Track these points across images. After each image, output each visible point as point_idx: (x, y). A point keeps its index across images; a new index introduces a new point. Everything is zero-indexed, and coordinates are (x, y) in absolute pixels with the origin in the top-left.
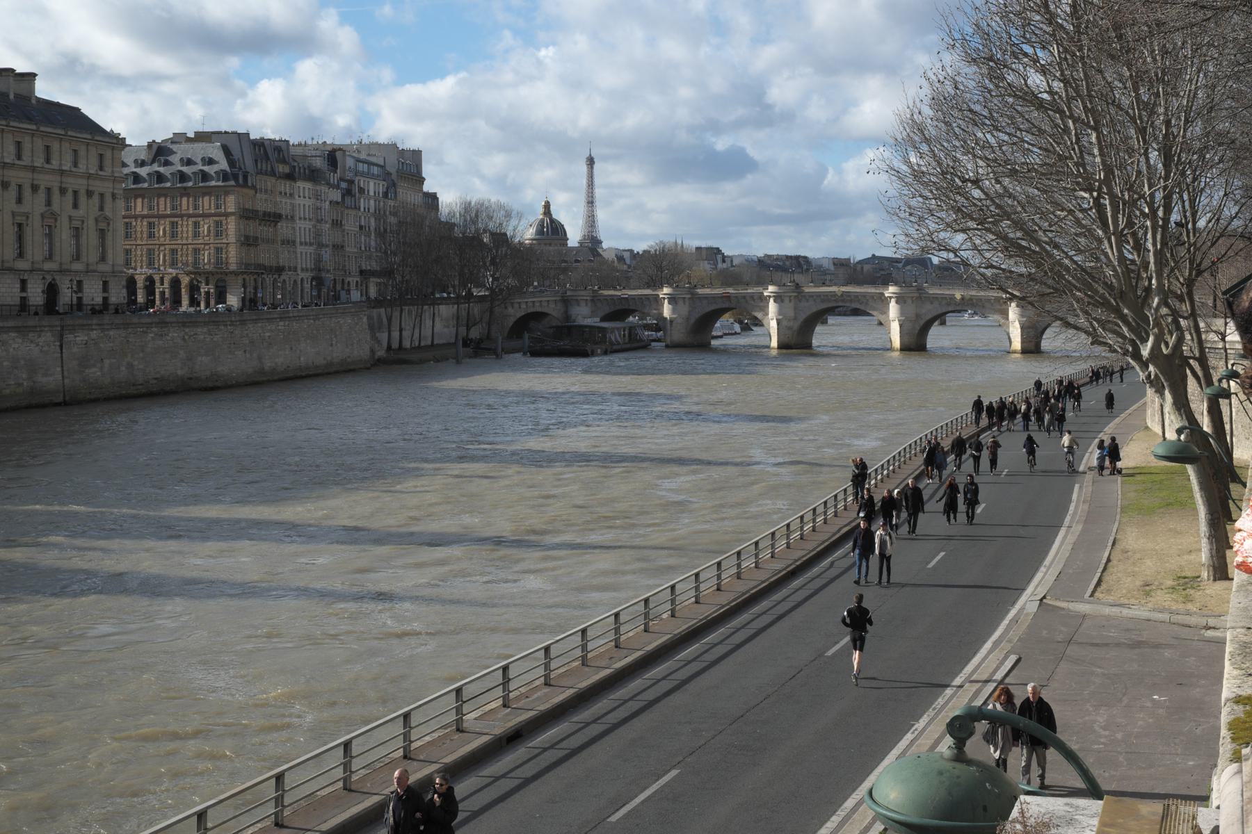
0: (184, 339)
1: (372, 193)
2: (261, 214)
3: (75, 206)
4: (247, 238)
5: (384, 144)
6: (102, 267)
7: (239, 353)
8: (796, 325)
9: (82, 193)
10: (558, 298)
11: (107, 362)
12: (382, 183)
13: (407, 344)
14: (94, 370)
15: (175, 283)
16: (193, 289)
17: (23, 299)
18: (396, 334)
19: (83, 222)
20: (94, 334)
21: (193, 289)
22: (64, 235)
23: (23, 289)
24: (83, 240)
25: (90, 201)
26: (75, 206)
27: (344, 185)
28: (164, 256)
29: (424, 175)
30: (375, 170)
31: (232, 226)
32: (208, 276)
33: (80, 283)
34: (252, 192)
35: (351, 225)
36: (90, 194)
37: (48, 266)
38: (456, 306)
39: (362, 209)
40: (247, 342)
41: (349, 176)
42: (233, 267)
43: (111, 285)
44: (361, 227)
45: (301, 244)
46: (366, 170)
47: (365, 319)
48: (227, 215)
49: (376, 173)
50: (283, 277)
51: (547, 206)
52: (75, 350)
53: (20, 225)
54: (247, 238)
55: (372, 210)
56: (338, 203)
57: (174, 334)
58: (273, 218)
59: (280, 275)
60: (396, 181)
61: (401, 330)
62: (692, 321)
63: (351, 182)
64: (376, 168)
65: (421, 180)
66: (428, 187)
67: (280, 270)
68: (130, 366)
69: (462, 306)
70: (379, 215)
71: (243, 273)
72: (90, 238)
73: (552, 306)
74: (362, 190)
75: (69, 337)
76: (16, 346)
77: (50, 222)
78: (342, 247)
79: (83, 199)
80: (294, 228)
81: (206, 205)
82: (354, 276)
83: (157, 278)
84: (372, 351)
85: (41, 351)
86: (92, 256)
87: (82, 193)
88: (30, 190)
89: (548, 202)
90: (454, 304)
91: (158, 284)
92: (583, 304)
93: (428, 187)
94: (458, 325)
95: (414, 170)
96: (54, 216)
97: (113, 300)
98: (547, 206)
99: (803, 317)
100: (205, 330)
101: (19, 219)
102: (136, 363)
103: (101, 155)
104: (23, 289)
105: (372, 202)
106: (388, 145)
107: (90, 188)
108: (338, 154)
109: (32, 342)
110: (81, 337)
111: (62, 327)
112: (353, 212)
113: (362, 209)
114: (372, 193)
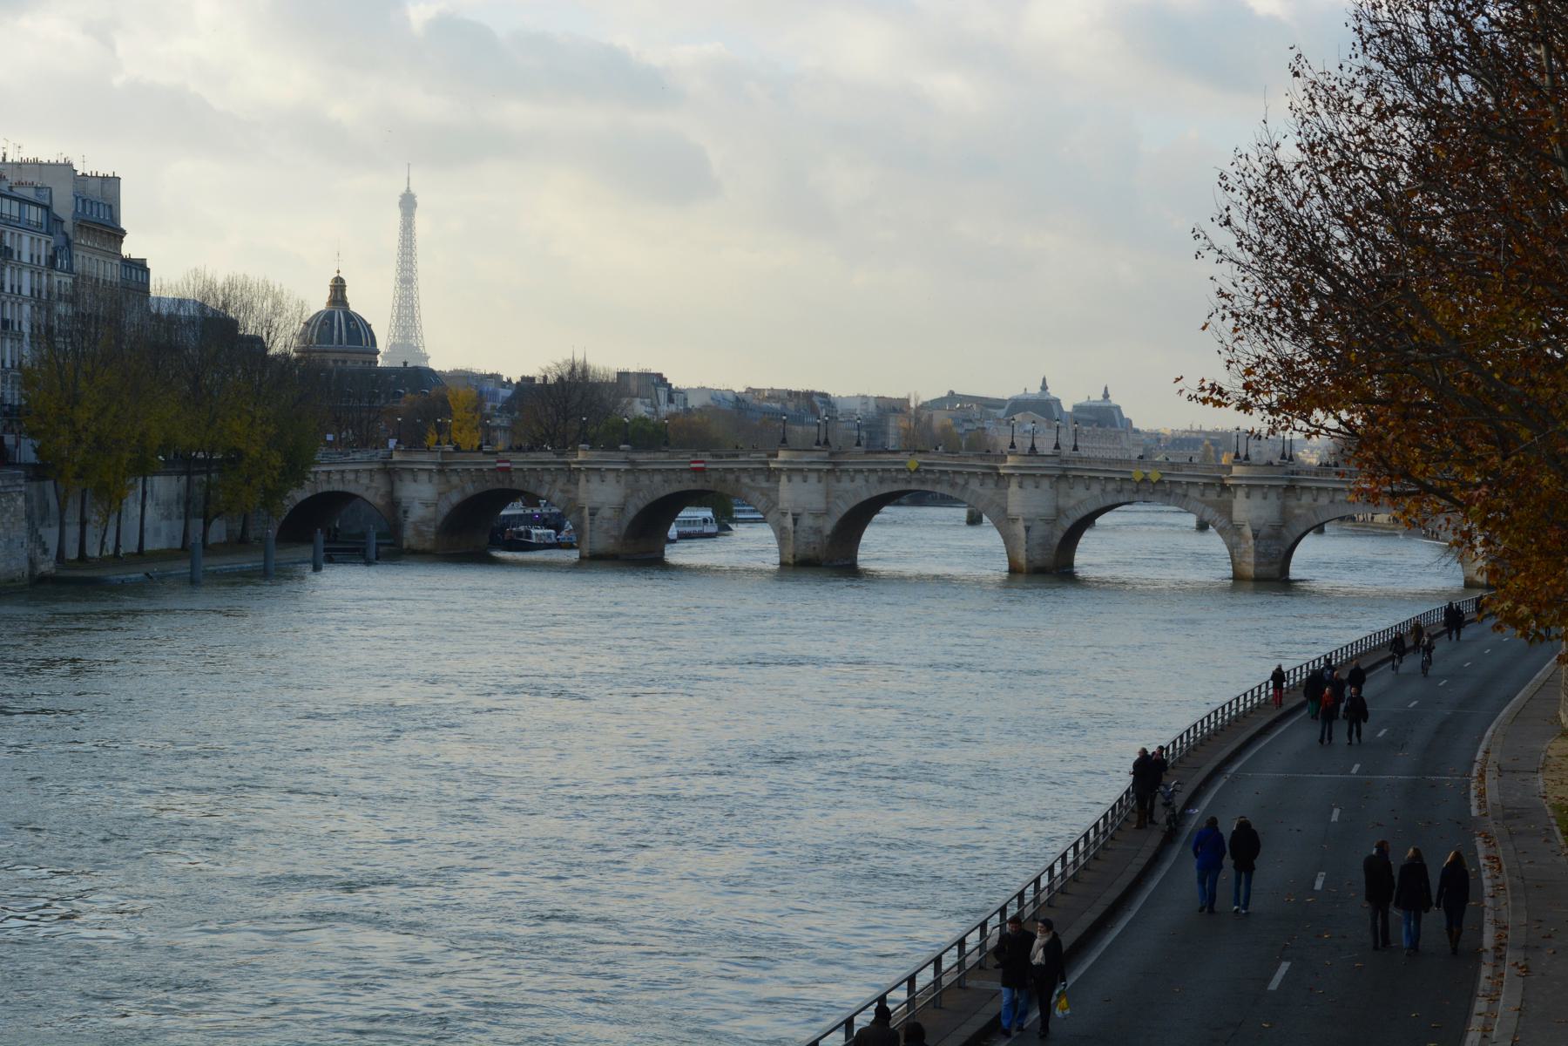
1: (26, 258)
5: (49, 164)
8: (829, 526)
10: (376, 466)
12: (44, 239)
13: (93, 551)
18: (73, 532)
29: (123, 225)
30: (34, 214)
38: (184, 478)
39: (8, 289)
46: (15, 213)
47: (20, 501)
49: (33, 218)
51: (338, 287)
55: (26, 291)
60: (71, 236)
61: (83, 523)
62: (632, 512)
64: (33, 209)
65: (119, 235)
66: (129, 249)
69: (196, 478)
70: (43, 301)
73: (364, 480)
84: (32, 563)
89: (342, 280)
90: (182, 474)
92: (424, 477)
93: (129, 249)
94: (187, 516)
95: (104, 216)
98: (338, 287)
99: (842, 508)
105: (26, 275)
106: (57, 165)
113: (8, 289)
114: (26, 258)
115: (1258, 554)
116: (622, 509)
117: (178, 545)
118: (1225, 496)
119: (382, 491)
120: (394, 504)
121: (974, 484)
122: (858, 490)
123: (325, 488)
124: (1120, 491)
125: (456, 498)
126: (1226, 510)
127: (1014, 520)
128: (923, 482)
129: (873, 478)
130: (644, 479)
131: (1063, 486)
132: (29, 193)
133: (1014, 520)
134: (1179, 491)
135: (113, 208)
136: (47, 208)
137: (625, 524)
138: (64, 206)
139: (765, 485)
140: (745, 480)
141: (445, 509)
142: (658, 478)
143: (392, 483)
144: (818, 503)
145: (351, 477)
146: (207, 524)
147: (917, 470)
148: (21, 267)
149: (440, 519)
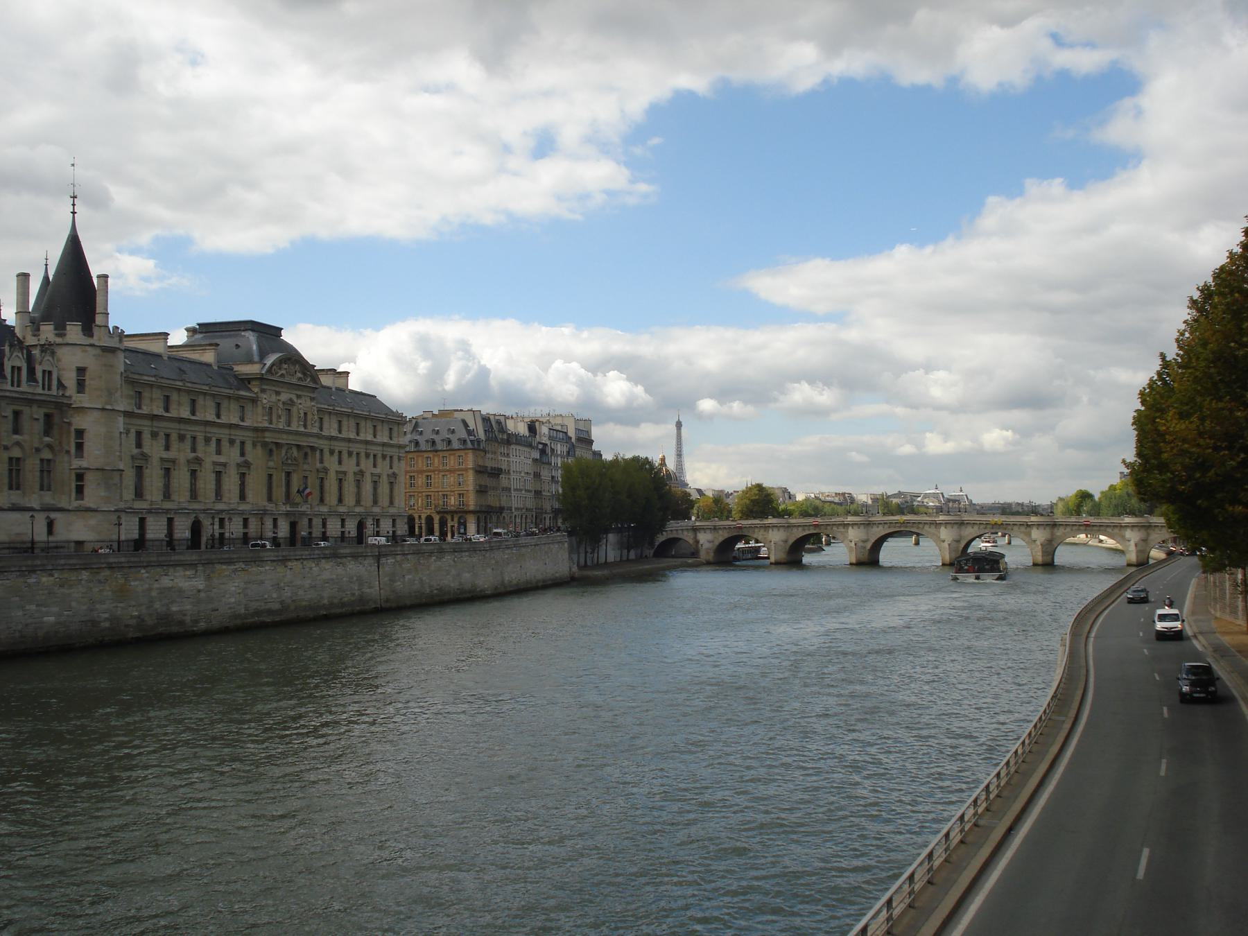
0: (454, 561)
1: (559, 452)
2: (489, 469)
3: (375, 466)
4: (480, 486)
6: (358, 510)
7: (489, 570)
8: (869, 545)
9: (380, 456)
11: (407, 577)
12: (565, 444)
13: (589, 563)
14: (399, 583)
15: (430, 520)
16: (443, 523)
17: (343, 533)
18: (582, 555)
19: (380, 477)
20: (399, 558)
21: (443, 523)
22: (367, 487)
23: (343, 526)
24: (380, 490)
25: (385, 462)
26: (375, 466)
27: (540, 446)
28: (422, 500)
31: (470, 477)
32: (453, 513)
33: (378, 520)
34: (483, 454)
35: (545, 474)
36: (384, 457)
37: (358, 510)
40: (494, 562)
41: (545, 440)
42: (472, 508)
43: (398, 521)
44: (553, 477)
45: (515, 490)
47: (566, 545)
48: (466, 470)
50: (503, 515)
52: (387, 569)
53: (341, 480)
54: (480, 486)
55: (559, 465)
56: (537, 459)
57: (448, 558)
58: (496, 473)
59: (501, 513)
61: (586, 552)
62: (791, 541)
63: (545, 445)
65: (591, 442)
66: (595, 447)
67: (501, 509)
68: (421, 580)
70: (567, 469)
71: (478, 512)
72: (384, 489)
74: (553, 450)
75: (383, 560)
76: (351, 566)
77: (359, 477)
78: (541, 492)
79: (379, 460)
80: (509, 479)
81: (452, 462)
82: (549, 513)
83: (416, 516)
85: (366, 570)
86: (383, 500)
87: (380, 456)
88: (347, 455)
91: (417, 521)
93: (595, 447)
96: (362, 473)
97: (399, 533)
100: (467, 554)
101: (341, 476)
102: (424, 578)
103: (391, 429)
104: (343, 526)
105: (559, 458)
107: (385, 453)
108: (537, 424)
109: (361, 563)
110: (391, 560)
111: (379, 552)
112: (546, 466)
114: (559, 452)
115: (1043, 552)
116: (786, 541)
117: (618, 559)
118: (1028, 529)
119: (692, 537)
120: (697, 542)
121: (927, 527)
122: (879, 532)
123: (671, 536)
124: (986, 528)
125: (721, 539)
126: (1029, 535)
127: (944, 541)
128: (906, 527)
129: (886, 526)
130: (795, 530)
131: (963, 527)
132: (559, 428)
133: (944, 541)
134: (1010, 527)
135: (588, 433)
136: (566, 433)
137: (788, 547)
138: (572, 433)
139: (843, 530)
140: (835, 528)
141: (717, 543)
142: (800, 529)
143: (696, 534)
144: (864, 537)
145: (680, 532)
146: (629, 552)
147: (904, 523)
148: (557, 456)
149: (715, 547)
